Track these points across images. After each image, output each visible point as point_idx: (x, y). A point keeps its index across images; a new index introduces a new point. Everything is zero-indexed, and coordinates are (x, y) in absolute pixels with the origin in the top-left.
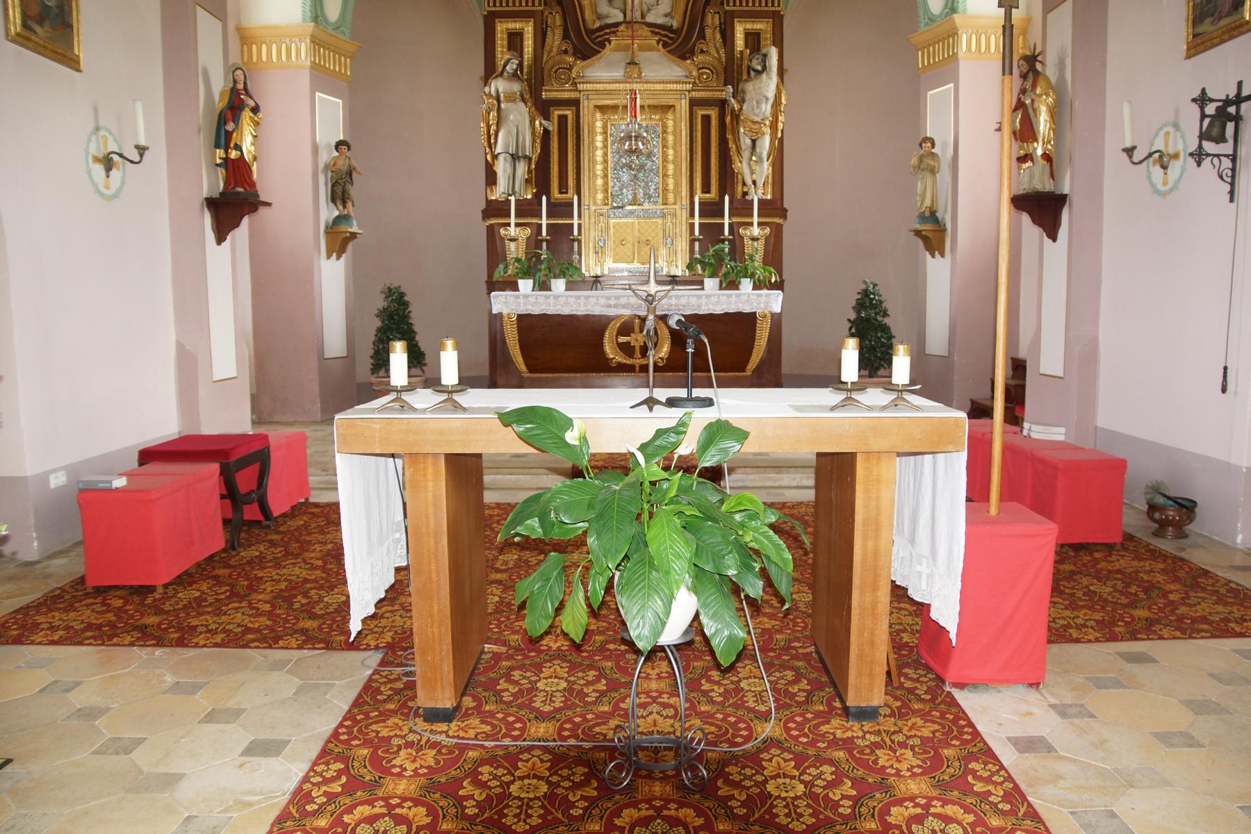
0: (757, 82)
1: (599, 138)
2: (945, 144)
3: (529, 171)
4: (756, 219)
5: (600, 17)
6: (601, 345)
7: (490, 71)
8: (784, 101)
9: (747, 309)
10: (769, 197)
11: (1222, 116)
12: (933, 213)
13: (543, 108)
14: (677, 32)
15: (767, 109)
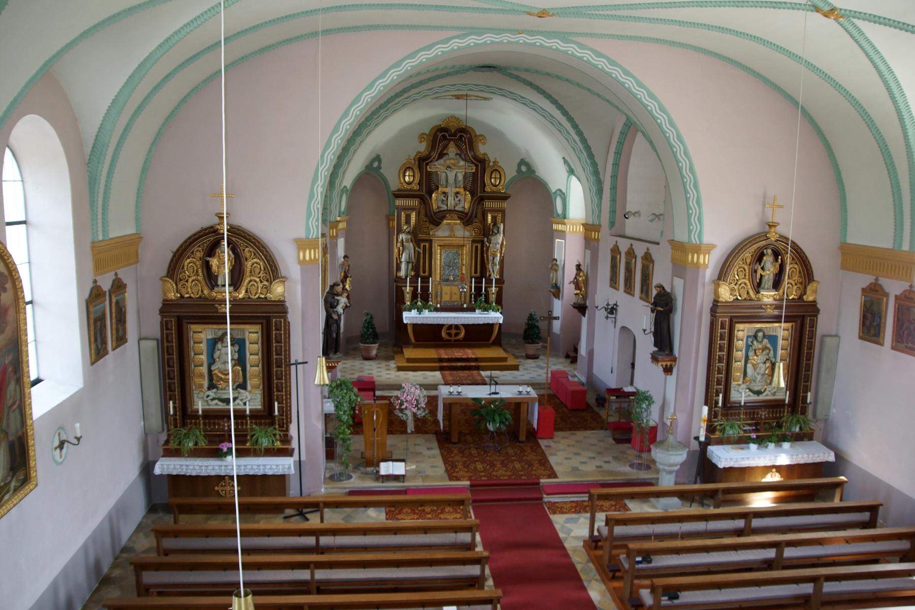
0: (495, 237)
1: (439, 256)
2: (561, 261)
3: (412, 266)
4: (494, 285)
5: (438, 207)
6: (441, 333)
7: (400, 231)
8: (504, 243)
9: (491, 322)
10: (498, 277)
11: (613, 308)
12: (556, 285)
13: (417, 241)
14: (467, 214)
15: (499, 246)
